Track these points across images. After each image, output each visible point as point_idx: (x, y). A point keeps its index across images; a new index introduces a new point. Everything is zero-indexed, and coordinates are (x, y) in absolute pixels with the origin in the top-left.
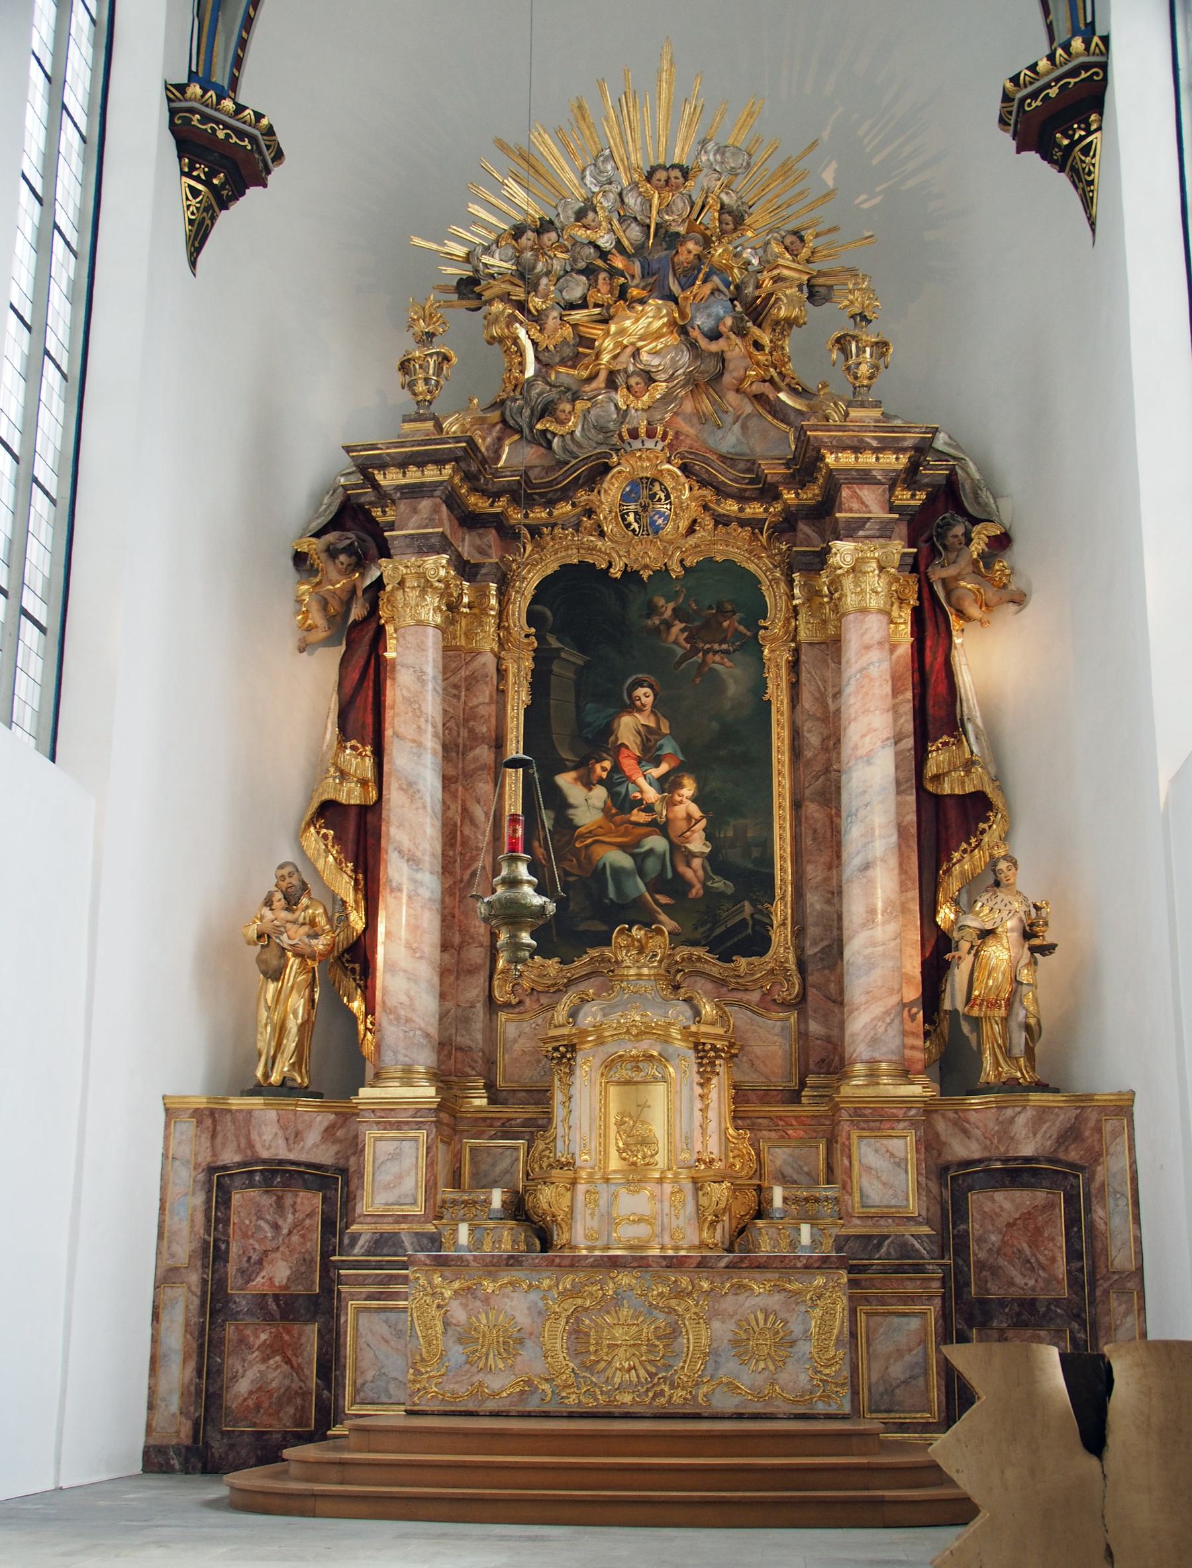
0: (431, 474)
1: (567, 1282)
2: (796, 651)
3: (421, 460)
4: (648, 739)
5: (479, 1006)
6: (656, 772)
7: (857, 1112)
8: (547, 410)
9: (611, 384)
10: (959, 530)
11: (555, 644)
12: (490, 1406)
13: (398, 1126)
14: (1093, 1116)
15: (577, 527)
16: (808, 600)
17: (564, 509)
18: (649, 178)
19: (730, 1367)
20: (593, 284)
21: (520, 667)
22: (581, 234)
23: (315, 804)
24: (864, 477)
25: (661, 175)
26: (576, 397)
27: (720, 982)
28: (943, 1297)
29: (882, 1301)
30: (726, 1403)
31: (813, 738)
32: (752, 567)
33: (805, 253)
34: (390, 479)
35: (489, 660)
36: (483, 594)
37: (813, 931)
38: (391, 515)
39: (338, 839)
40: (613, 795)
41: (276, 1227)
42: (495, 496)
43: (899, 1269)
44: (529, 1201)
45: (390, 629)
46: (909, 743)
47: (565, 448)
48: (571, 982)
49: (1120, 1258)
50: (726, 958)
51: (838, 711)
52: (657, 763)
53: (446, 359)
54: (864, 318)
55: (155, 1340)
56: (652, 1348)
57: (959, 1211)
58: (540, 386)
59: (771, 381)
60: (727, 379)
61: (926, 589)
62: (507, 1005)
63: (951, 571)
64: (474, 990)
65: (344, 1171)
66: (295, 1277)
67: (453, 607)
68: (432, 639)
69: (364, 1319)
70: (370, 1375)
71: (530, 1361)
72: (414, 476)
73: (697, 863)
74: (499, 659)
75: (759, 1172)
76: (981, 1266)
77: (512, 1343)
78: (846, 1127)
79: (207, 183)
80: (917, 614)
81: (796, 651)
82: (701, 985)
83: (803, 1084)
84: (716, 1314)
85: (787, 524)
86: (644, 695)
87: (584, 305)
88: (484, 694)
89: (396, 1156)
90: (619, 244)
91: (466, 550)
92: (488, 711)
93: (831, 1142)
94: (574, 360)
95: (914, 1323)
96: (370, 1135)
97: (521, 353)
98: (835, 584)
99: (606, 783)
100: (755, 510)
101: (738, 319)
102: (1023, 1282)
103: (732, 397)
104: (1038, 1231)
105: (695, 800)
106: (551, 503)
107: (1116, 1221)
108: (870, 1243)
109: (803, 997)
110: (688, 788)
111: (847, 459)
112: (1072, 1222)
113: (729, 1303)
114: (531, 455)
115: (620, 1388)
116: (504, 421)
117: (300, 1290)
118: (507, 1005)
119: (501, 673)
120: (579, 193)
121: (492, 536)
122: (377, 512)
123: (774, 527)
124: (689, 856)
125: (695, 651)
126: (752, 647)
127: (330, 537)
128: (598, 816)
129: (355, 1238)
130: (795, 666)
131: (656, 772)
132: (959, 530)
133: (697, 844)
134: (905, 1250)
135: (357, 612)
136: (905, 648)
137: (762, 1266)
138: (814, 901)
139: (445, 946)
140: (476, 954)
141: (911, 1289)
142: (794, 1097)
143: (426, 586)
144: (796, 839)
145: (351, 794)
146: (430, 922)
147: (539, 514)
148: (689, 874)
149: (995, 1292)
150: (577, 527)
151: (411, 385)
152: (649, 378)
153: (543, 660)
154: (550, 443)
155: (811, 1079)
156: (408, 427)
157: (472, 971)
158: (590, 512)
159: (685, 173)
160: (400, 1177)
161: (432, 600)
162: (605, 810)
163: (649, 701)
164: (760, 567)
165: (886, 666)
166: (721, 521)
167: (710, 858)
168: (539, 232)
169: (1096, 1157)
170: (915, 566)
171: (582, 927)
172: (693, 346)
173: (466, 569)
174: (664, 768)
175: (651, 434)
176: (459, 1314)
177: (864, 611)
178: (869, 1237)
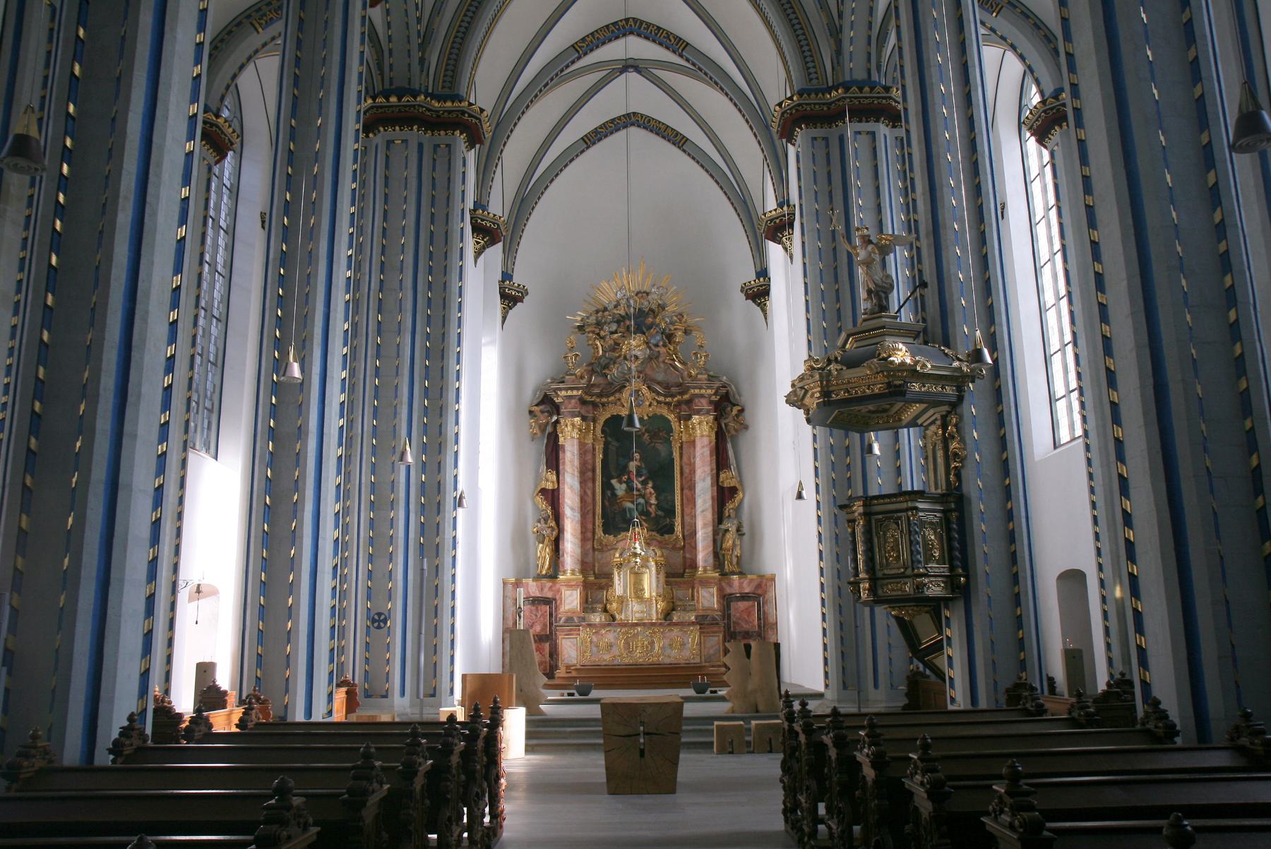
0: (575, 393)
1: (623, 630)
2: (682, 443)
3: (572, 389)
4: (638, 469)
5: (591, 551)
6: (641, 479)
7: (701, 581)
8: (606, 367)
9: (625, 358)
10: (729, 409)
11: (609, 439)
12: (604, 663)
13: (571, 586)
14: (764, 581)
15: (616, 404)
16: (685, 428)
17: (612, 398)
18: (637, 295)
19: (668, 651)
20: (619, 326)
21: (599, 447)
22: (615, 312)
23: (539, 489)
24: (702, 396)
25: (640, 295)
26: (615, 363)
27: (660, 542)
28: (724, 632)
29: (708, 633)
30: (667, 661)
31: (686, 470)
32: (669, 417)
33: (684, 320)
34: (563, 393)
35: (591, 445)
36: (589, 426)
37: (687, 528)
38: (560, 400)
39: (546, 499)
40: (628, 486)
41: (536, 616)
42: (592, 396)
43: (712, 624)
44: (608, 606)
45: (560, 435)
46: (715, 471)
47: (611, 378)
48: (617, 542)
49: (771, 620)
50: (662, 535)
51: (695, 463)
52: (641, 476)
53: (577, 355)
54: (702, 347)
55: (503, 648)
56: (647, 647)
57: (729, 607)
58: (603, 359)
59: (674, 360)
60: (661, 359)
61: (719, 426)
62: (598, 550)
63: (727, 421)
64: (589, 545)
65: (555, 599)
66: (542, 630)
67: (580, 430)
68: (576, 442)
69: (564, 641)
70: (566, 656)
71: (615, 651)
72: (570, 393)
73: (653, 507)
74: (593, 445)
75: (673, 598)
76: (734, 622)
77: (610, 646)
78: (696, 585)
79: (508, 306)
80: (717, 433)
81: (682, 443)
82: (654, 542)
83: (684, 572)
84: (664, 637)
85: (679, 404)
86: (637, 456)
87: (616, 332)
88: (589, 457)
89: (571, 595)
90: (627, 314)
91: (583, 412)
92: (590, 461)
93: (693, 588)
94: (614, 350)
95: (716, 638)
96: (563, 589)
97: (597, 348)
98: (693, 429)
99: (627, 483)
100: (669, 400)
101: (664, 342)
102: (746, 627)
103: (662, 365)
104: (750, 613)
105: (652, 488)
106: (609, 397)
107: (771, 610)
108: (705, 617)
109: (684, 546)
110: (650, 485)
111: (697, 391)
112: (759, 610)
113: (668, 635)
114: (600, 380)
115: (639, 658)
116: (593, 369)
117: (542, 633)
118: (598, 550)
119: (594, 449)
120: (615, 299)
121: (590, 407)
122: (555, 399)
123: (675, 405)
124: (651, 505)
125: (652, 442)
126: (668, 442)
127: (542, 407)
128: (624, 492)
129: (560, 619)
130: (681, 448)
131: (641, 479)
132: (729, 409)
133: (653, 501)
134: (714, 619)
135: (549, 429)
136: (713, 443)
137: (676, 624)
138: (687, 519)
139: (582, 532)
140: (589, 535)
141: (716, 629)
142: (682, 575)
143: (573, 425)
144: (682, 499)
145: (550, 486)
146: (578, 527)
147: (604, 400)
148: (651, 510)
149: (738, 629)
150: (616, 404)
151: (568, 364)
152: (637, 357)
153: (606, 444)
154: (607, 377)
155: (687, 571)
156: (567, 377)
157: (588, 540)
158: (619, 399)
159: (648, 294)
160: (572, 601)
161: (576, 431)
162: (626, 491)
163: (638, 457)
164: (671, 417)
165: (708, 452)
166: (659, 402)
167: (657, 505)
168: (603, 312)
169: (765, 592)
170: (716, 419)
171: (620, 526)
172: (650, 348)
173: (584, 419)
174: (643, 478)
175: (639, 377)
176: (595, 639)
177: (702, 436)
178: (703, 616)
